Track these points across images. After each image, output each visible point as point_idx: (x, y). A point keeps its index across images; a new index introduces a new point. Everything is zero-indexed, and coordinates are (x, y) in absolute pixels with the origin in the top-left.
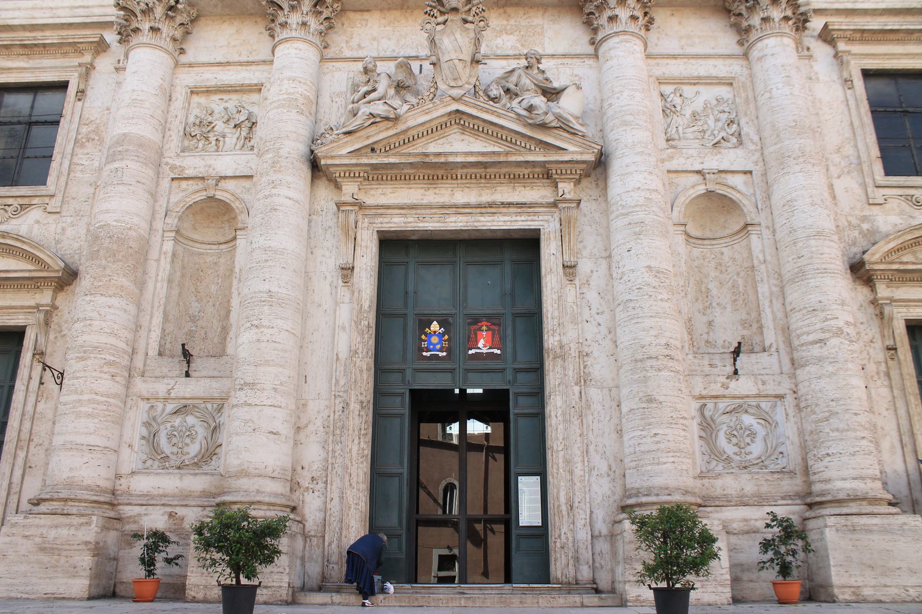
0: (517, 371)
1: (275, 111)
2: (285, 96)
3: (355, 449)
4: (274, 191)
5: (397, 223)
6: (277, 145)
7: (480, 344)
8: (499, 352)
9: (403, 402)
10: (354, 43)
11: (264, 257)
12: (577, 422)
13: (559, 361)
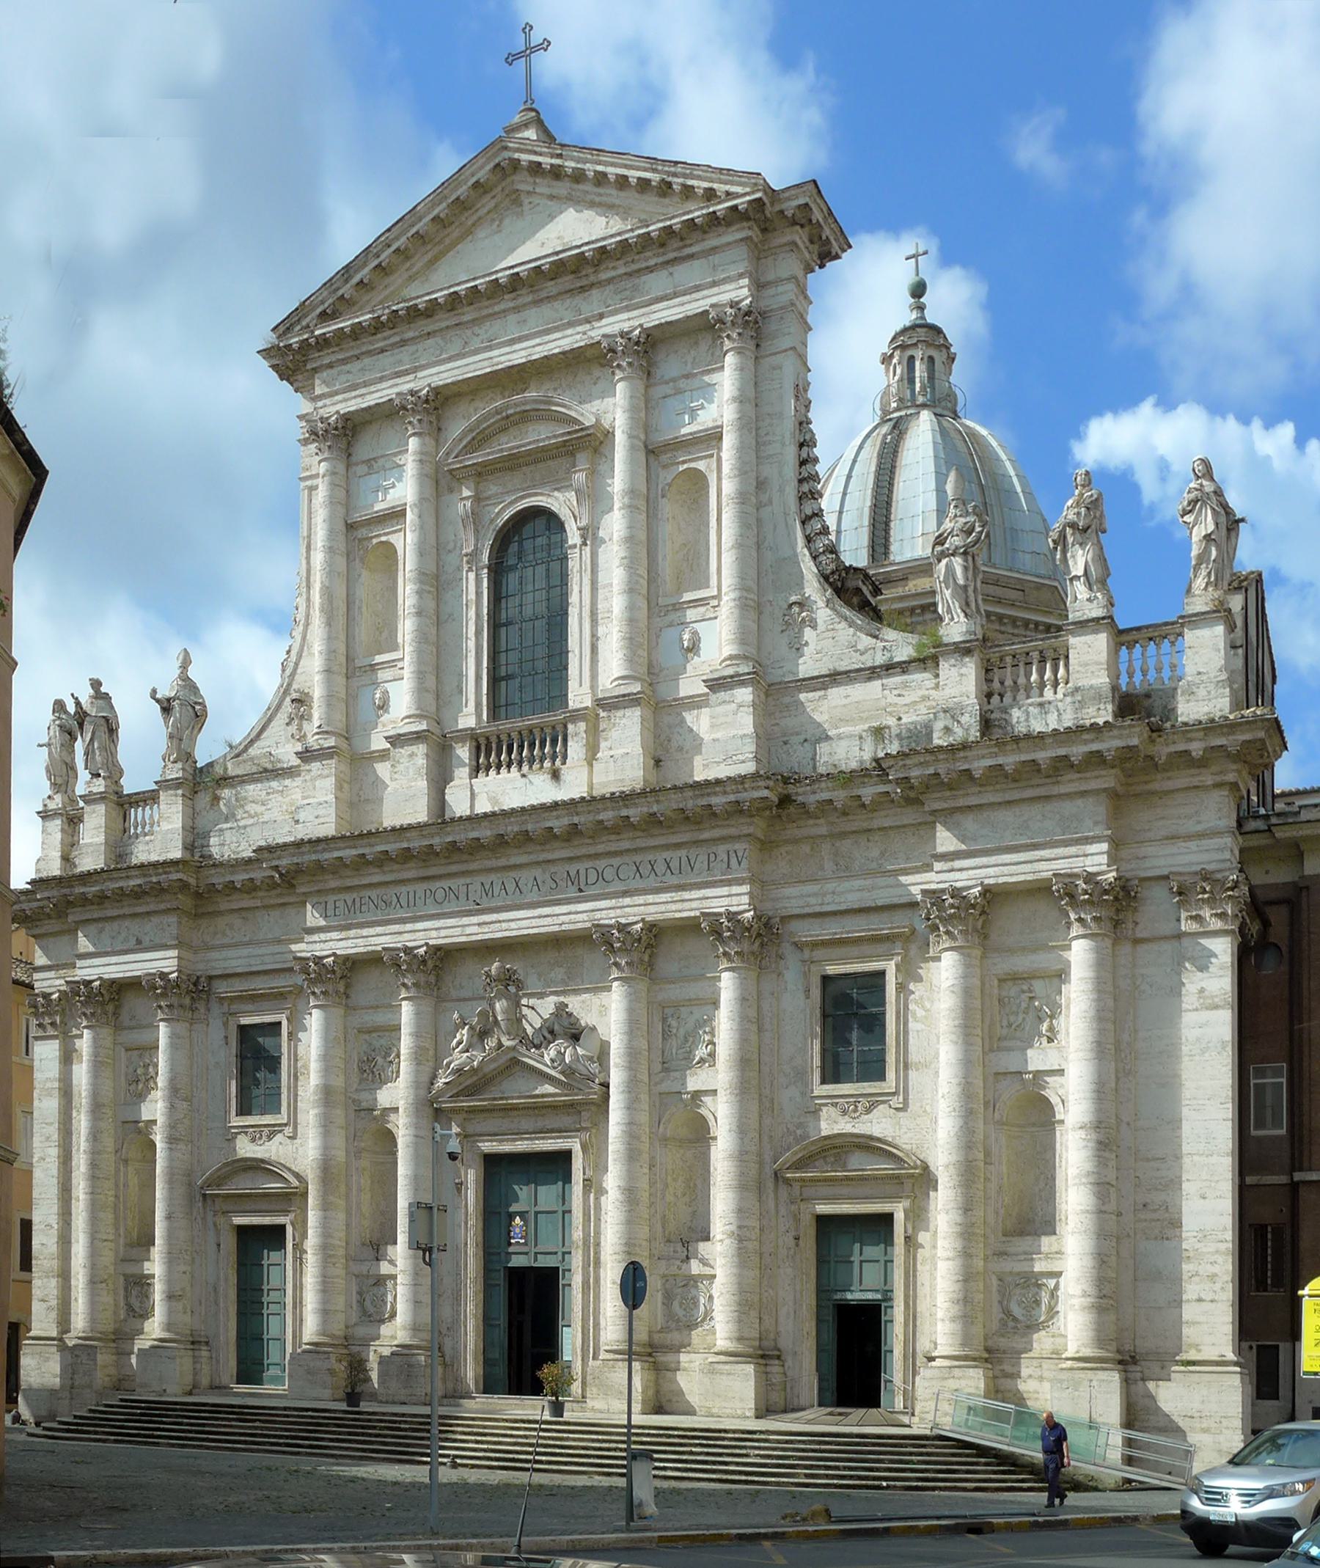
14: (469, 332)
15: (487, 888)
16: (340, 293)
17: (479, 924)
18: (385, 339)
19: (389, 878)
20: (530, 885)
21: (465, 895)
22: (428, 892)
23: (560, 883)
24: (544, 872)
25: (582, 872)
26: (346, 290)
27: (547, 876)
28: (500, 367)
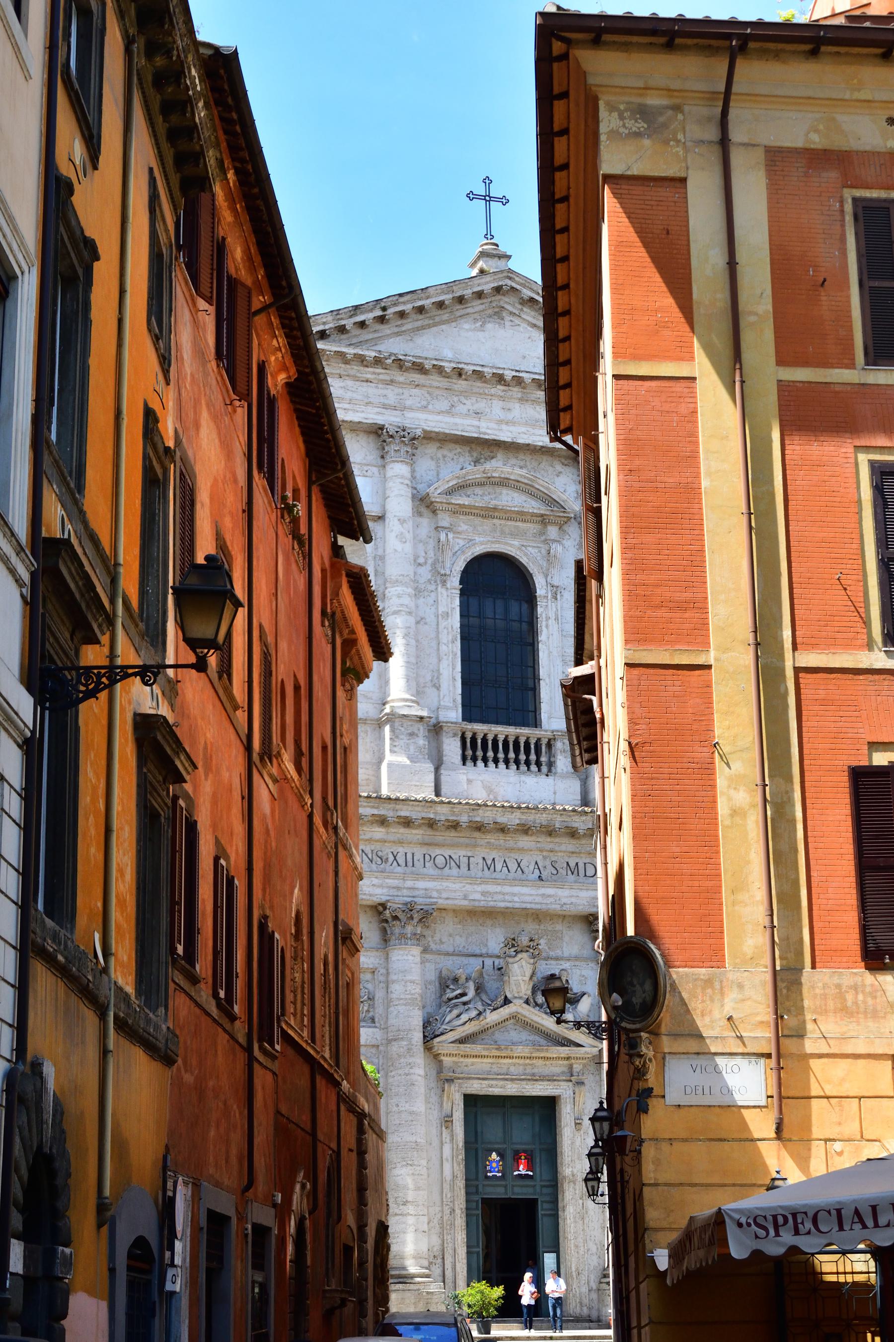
0: (542, 1186)
1: (403, 1007)
2: (410, 996)
3: (460, 1238)
4: (412, 1071)
5: (477, 1087)
6: (409, 1036)
7: (521, 1169)
8: (531, 1173)
9: (477, 1205)
10: (437, 937)
11: (410, 1118)
12: (581, 1222)
13: (572, 1185)
14: (456, 399)
15: (489, 862)
16: (343, 322)
17: (483, 894)
18: (374, 373)
19: (391, 837)
20: (531, 867)
21: (466, 865)
22: (427, 857)
23: (560, 870)
24: (545, 858)
25: (581, 866)
26: (349, 323)
27: (548, 863)
28: (487, 437)
